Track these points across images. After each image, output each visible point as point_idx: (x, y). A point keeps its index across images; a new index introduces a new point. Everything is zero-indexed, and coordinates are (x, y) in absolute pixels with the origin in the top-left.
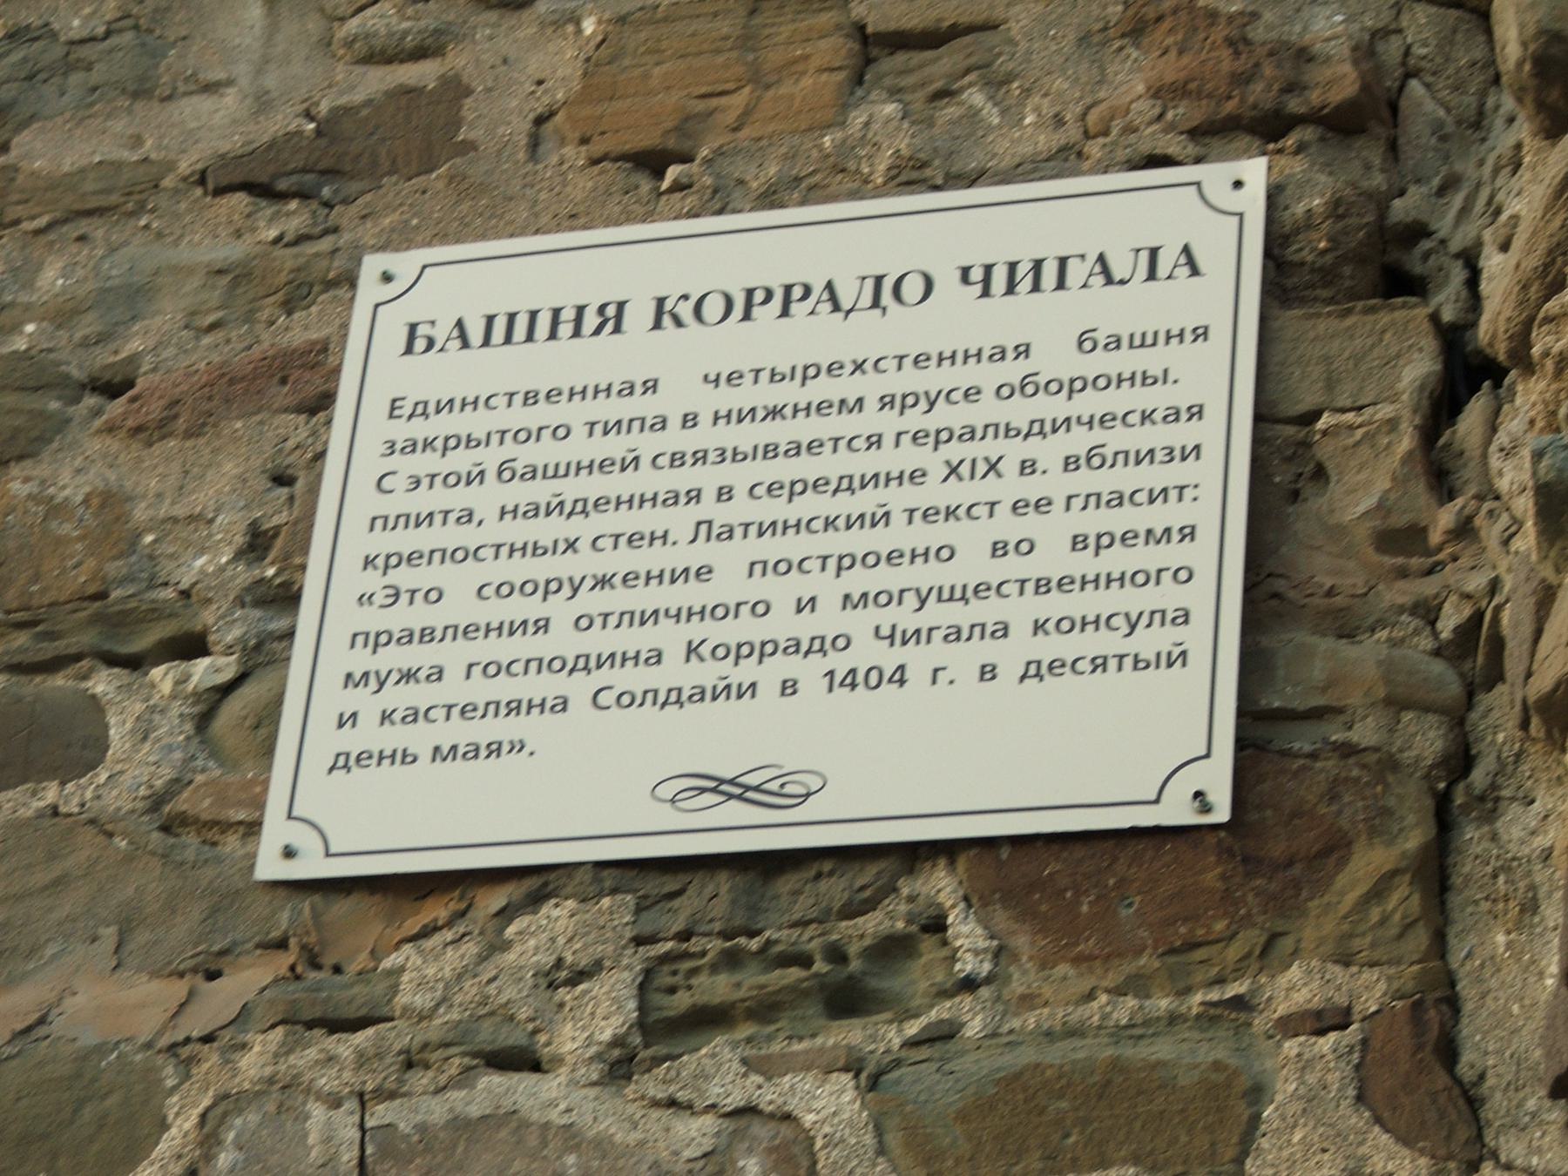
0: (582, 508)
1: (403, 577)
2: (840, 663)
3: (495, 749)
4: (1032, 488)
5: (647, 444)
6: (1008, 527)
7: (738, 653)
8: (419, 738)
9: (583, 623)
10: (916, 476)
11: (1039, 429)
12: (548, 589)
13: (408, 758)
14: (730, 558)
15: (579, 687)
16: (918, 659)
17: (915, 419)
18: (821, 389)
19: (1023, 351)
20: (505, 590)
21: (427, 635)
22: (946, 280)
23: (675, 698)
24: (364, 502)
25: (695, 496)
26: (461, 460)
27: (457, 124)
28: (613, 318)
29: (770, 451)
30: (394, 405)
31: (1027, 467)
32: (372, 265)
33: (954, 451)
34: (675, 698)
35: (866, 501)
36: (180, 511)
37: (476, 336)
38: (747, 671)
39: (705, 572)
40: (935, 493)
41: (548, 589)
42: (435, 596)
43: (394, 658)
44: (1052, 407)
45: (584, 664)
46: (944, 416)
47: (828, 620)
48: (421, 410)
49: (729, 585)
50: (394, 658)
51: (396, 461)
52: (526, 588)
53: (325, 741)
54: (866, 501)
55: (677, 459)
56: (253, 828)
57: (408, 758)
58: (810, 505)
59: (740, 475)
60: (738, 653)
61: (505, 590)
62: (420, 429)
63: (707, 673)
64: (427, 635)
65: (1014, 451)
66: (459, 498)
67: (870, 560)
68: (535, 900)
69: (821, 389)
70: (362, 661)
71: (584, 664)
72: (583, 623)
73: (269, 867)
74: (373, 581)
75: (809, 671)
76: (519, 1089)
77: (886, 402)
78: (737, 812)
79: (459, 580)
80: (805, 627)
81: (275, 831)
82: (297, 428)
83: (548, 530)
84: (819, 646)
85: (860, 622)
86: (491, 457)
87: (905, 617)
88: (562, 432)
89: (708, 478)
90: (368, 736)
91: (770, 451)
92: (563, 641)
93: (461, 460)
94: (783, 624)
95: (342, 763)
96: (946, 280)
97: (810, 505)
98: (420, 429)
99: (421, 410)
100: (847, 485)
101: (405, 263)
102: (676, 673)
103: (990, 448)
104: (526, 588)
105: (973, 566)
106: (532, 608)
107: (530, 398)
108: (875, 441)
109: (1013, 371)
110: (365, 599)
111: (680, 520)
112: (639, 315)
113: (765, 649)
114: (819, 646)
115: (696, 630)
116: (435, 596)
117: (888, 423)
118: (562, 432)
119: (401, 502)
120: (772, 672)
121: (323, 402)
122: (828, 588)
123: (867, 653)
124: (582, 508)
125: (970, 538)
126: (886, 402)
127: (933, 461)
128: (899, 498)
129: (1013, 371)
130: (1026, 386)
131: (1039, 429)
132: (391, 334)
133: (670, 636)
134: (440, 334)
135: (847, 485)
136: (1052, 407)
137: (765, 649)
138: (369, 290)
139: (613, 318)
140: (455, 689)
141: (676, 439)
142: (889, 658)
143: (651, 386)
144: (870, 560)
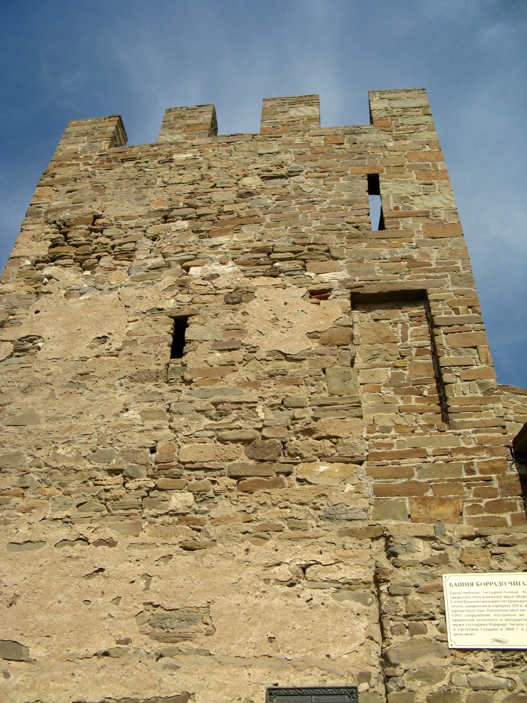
0: (474, 607)
1: (456, 613)
2: (507, 627)
3: (471, 634)
4: (522, 608)
5: (480, 600)
6: (522, 613)
7: (495, 625)
8: (463, 632)
9: (478, 620)
10: (509, 606)
11: (521, 602)
12: (473, 616)
13: (462, 635)
14: (492, 613)
15: (479, 628)
16: (515, 627)
17: (508, 599)
18: (497, 595)
19: (517, 592)
20: (468, 616)
21: (461, 620)
22: (507, 583)
23: (489, 630)
24: (450, 604)
25: (486, 606)
26: (459, 600)
27: (448, 559)
28: (472, 584)
29: (493, 602)
30: (450, 593)
31: (521, 606)
32: (444, 575)
33: (513, 603)
34: (489, 630)
35: (505, 608)
36: (428, 602)
37: (457, 585)
38: (496, 627)
39: (489, 615)
40: (512, 608)
41: (473, 616)
42: (460, 616)
43: (458, 623)
44: (522, 599)
45: (479, 625)
46: (511, 599)
47: (504, 622)
48: (453, 593)
49: (492, 617)
50: (458, 623)
51: (452, 599)
52: (471, 616)
53: (453, 632)
54: (505, 608)
55: (483, 602)
56: (447, 641)
57: (462, 635)
58: (498, 608)
59: (491, 604)
60: (495, 625)
61: (468, 616)
62: (454, 596)
63: (493, 627)
64: (461, 620)
65: (519, 604)
66: (460, 604)
67: (507, 615)
68: (480, 652)
69: (497, 595)
70: (454, 623)
71: (479, 625)
72: (478, 620)
73: (450, 647)
74: (453, 613)
75: (503, 627)
76: (483, 673)
77: (504, 597)
78: (499, 644)
79: (463, 614)
80: (502, 622)
81: (450, 643)
82: (440, 594)
83: (471, 609)
84: (504, 625)
85: (508, 622)
86: (463, 600)
87: (512, 622)
88: (470, 597)
89: (488, 604)
90: (457, 632)
91: (493, 602)
92: (475, 622)
93: (459, 600)
94: (499, 622)
95: (455, 635)
96: (507, 583)
97: (498, 608)
98: (454, 596)
99: (453, 593)
100: (502, 606)
101: (447, 575)
102: (489, 627)
103: (517, 603)
104: (471, 616)
105: (518, 617)
106: (471, 618)
107: (465, 593)
108: (504, 601)
109: (517, 594)
110: (453, 615)
111: (485, 609)
112: (475, 584)
113: (498, 625)
114: (504, 625)
115: (490, 622)
116: (460, 616)
117: (505, 599)
118: (470, 597)
119: (454, 604)
120: (500, 627)
121: (442, 591)
122: (504, 618)
123: (509, 626)
124: (474, 607)
125: (517, 613)
126: (504, 597)
127: (511, 604)
128: (508, 608)
129: (517, 594)
130: (518, 596)
131: (521, 602)
132: (448, 585)
133: (488, 623)
134: (454, 584)
135: (502, 606)
136: (522, 599)
137: (498, 625)
138: (444, 579)
139: (472, 584)
140: (465, 627)
141: (482, 599)
142: (512, 627)
143: (478, 593)
144: (507, 615)
